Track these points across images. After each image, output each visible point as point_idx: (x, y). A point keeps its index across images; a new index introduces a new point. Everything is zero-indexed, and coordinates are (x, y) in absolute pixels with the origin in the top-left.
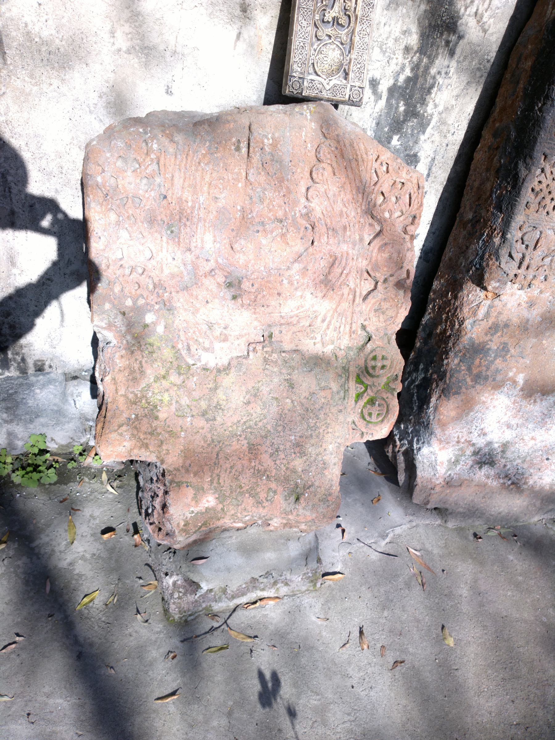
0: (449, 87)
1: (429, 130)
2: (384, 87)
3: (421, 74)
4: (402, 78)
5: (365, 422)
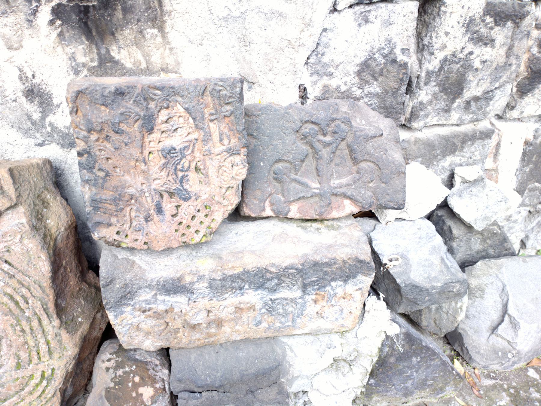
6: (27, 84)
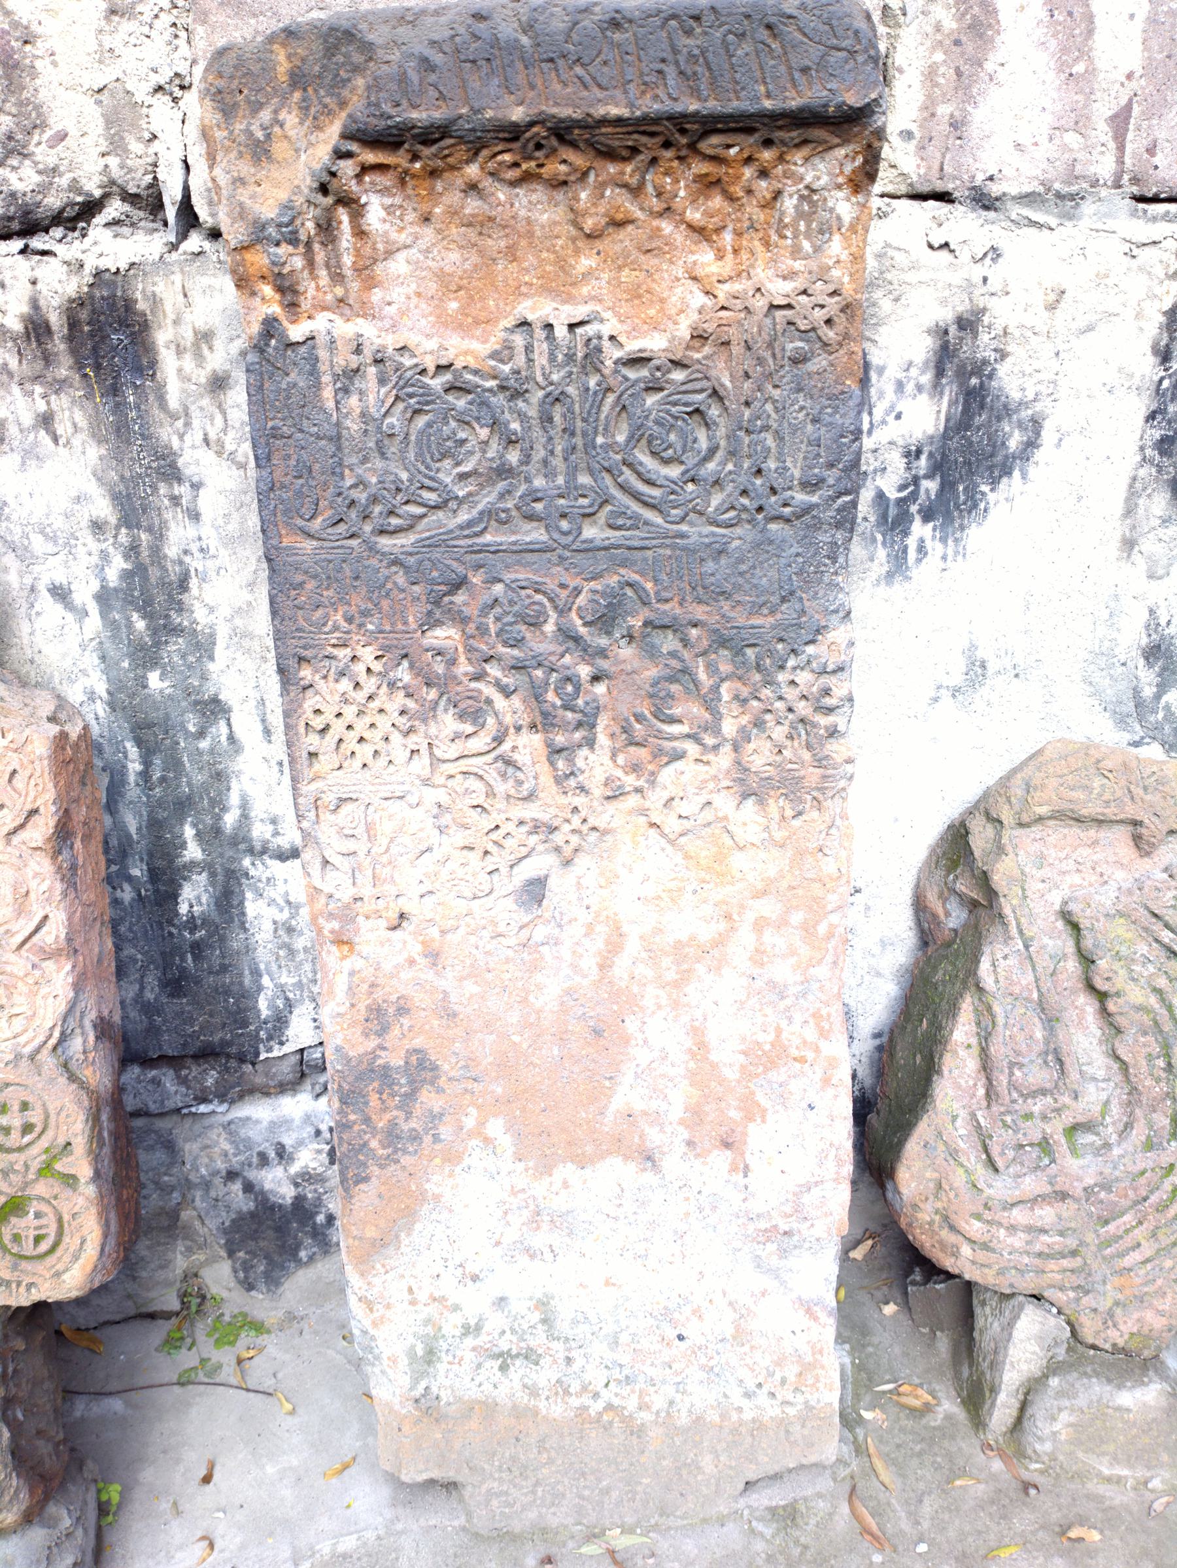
0: (222, 572)
1: (219, 651)
2: (84, 593)
3: (148, 560)
4: (113, 576)
5: (8, 1257)
6: (1154, 636)
